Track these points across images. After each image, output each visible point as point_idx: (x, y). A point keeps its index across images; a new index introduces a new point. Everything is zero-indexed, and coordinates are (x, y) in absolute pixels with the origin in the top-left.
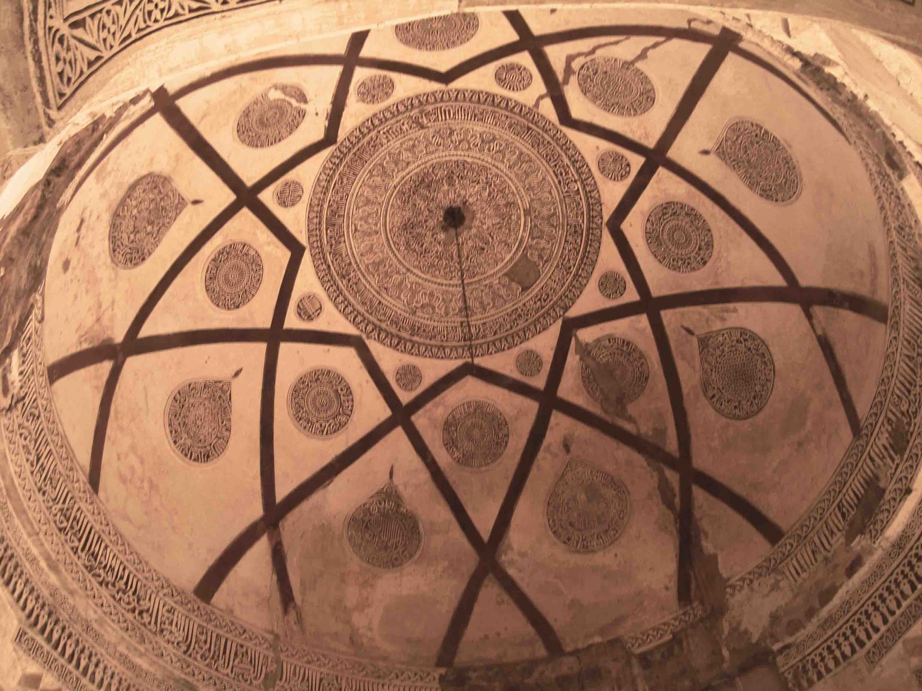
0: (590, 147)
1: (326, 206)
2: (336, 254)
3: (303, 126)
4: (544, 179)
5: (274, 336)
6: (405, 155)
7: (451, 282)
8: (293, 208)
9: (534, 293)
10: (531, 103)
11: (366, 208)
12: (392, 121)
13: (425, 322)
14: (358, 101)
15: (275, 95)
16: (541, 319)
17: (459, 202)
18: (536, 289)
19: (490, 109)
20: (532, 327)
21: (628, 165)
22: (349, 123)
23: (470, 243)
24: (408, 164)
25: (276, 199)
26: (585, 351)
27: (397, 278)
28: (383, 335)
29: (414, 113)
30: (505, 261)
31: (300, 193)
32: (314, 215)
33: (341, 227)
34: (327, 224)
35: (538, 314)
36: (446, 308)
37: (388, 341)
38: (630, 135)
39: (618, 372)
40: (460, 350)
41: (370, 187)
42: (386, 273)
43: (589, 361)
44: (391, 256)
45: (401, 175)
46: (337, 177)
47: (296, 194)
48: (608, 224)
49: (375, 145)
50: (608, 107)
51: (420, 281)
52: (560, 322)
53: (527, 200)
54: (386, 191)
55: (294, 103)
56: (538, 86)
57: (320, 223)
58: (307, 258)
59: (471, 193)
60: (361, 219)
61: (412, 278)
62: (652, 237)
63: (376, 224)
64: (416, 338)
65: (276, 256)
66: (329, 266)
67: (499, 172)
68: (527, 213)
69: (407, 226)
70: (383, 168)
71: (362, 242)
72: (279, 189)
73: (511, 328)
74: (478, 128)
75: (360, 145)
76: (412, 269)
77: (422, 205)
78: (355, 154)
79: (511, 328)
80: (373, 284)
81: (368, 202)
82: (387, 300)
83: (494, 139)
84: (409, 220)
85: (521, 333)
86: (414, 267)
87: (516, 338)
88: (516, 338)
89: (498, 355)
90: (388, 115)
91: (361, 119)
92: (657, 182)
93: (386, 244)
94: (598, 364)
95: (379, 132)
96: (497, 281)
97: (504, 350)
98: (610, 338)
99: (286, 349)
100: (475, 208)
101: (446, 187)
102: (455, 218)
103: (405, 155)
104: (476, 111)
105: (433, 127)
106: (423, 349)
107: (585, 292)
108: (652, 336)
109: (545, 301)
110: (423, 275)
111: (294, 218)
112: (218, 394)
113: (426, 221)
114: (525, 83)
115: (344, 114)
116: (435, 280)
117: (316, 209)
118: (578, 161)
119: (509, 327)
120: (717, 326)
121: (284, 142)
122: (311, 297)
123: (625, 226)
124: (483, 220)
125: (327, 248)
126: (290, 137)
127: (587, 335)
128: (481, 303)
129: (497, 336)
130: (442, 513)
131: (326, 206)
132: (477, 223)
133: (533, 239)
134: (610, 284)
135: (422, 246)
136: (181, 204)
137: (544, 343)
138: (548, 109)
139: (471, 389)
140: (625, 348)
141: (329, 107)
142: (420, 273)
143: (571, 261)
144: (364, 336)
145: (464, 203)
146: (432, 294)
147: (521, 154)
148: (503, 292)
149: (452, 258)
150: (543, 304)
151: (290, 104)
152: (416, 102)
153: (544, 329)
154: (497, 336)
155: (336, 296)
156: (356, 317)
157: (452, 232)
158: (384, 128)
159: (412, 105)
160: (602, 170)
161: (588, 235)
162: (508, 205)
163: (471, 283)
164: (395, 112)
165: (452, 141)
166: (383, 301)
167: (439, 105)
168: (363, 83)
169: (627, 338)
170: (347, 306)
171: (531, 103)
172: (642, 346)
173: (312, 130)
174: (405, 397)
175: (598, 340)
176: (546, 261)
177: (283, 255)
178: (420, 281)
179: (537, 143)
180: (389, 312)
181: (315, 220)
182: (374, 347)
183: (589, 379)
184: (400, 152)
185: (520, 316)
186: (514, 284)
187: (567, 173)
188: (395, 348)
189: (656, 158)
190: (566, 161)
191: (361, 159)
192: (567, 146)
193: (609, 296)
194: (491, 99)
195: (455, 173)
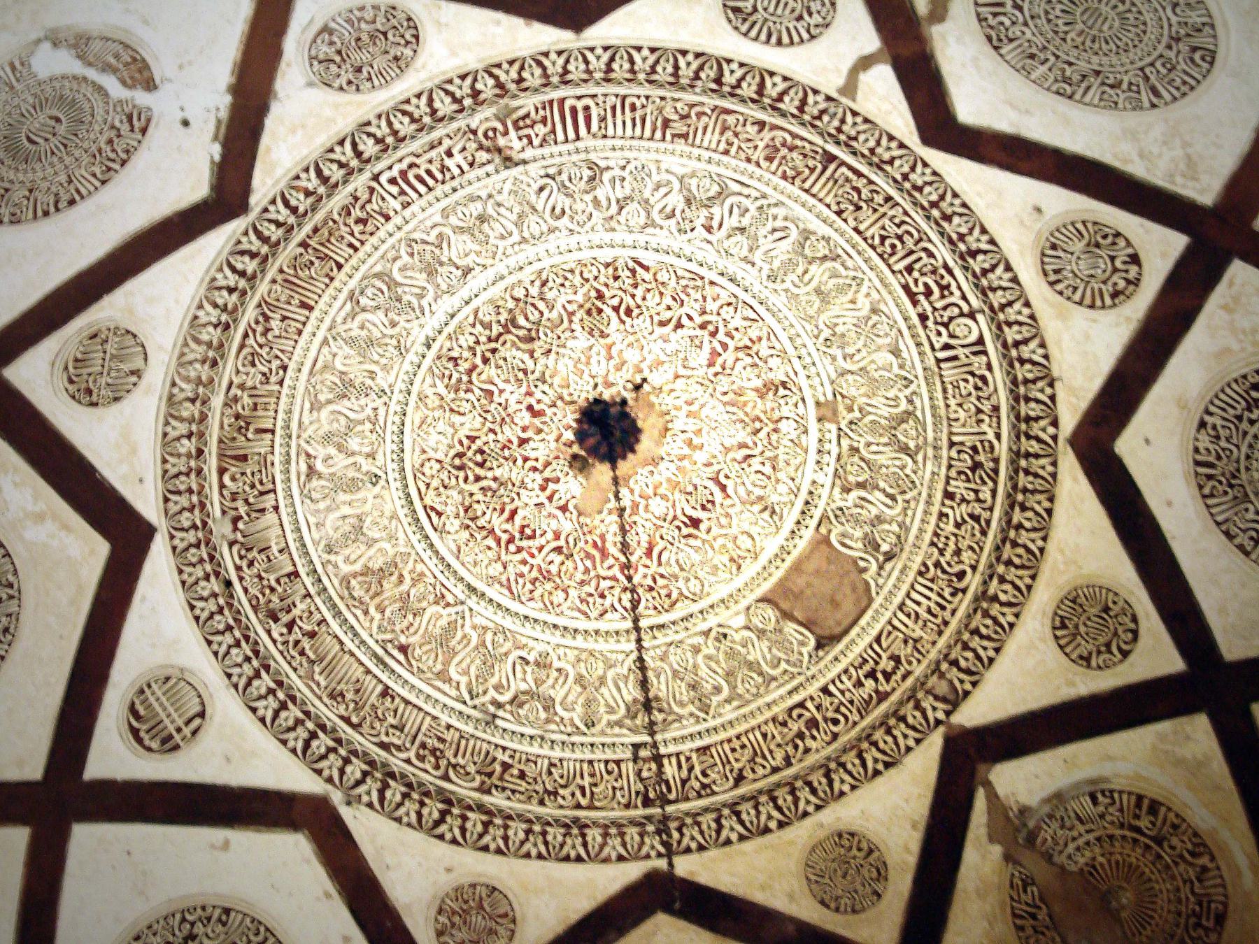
0: (1013, 208)
1: (217, 401)
2: (248, 547)
3: (140, 161)
4: (874, 311)
6: (460, 247)
7: (603, 625)
8: (116, 407)
9: (857, 650)
10: (831, 83)
11: (341, 406)
12: (415, 146)
13: (525, 747)
14: (311, 84)
15: (53, 63)
16: (879, 735)
18: (858, 643)
19: (711, 101)
20: (851, 759)
21: (1135, 259)
22: (281, 155)
23: (658, 506)
24: (467, 272)
25: (62, 382)
26: (1017, 831)
27: (435, 617)
28: (395, 792)
29: (482, 118)
30: (763, 559)
31: (138, 363)
32: (183, 428)
33: (265, 463)
34: (221, 456)
35: (868, 721)
36: (588, 703)
37: (411, 806)
38: (1137, 169)
39: (1127, 898)
40: (632, 832)
41: (351, 342)
42: (405, 599)
43: (1033, 864)
44: (420, 547)
45: (448, 303)
46: (250, 314)
47: (126, 367)
48: (1075, 442)
49: (364, 219)
50: (1068, 87)
51: (508, 622)
52: (935, 742)
53: (826, 369)
54: (402, 350)
55: (112, 85)
57: (200, 452)
58: (159, 564)
60: (327, 438)
61: (485, 614)
62: (1215, 476)
63: (372, 456)
64: (496, 800)
66: (228, 584)
67: (742, 295)
68: (826, 412)
69: (469, 460)
70: (392, 284)
71: (329, 510)
72: (73, 351)
73: (788, 761)
74: (674, 160)
75: (319, 216)
76: (481, 586)
77: (513, 395)
78: (304, 244)
79: (788, 761)
80: (365, 636)
81: (346, 387)
82: (410, 684)
83: (722, 194)
84: (472, 439)
85: (817, 778)
86: (491, 580)
87: (804, 794)
88: (804, 794)
89: (747, 846)
90: (404, 126)
91: (324, 139)
92: (1225, 308)
93: (401, 513)
94: (1062, 868)
95: (376, 178)
96: (740, 621)
97: (767, 830)
98: (1096, 791)
99: (89, 841)
100: (667, 401)
101: (582, 341)
102: (607, 431)
103: (460, 247)
104: (669, 113)
105: (541, 158)
106: (517, 830)
107: (1013, 645)
108: (1229, 783)
109: (888, 676)
110: (515, 606)
111: (123, 443)
113: (523, 442)
115: (269, 122)
116: (552, 619)
117: (188, 410)
118: (978, 252)
119: (779, 761)
121: (82, 208)
122: (171, 680)
123: (1129, 446)
125: (221, 529)
126: (106, 195)
127: (1020, 781)
128: (693, 687)
129: (742, 790)
131: (217, 401)
132: (673, 446)
133: (847, 490)
134: (1086, 623)
135: (514, 513)
137: (891, 808)
138: (884, 100)
140: (1144, 823)
141: (224, 101)
142: (507, 602)
143: (967, 556)
144: (337, 797)
145: (637, 388)
146: (542, 664)
147: (806, 234)
148: (759, 652)
149: (604, 554)
150: (884, 687)
151: (100, 89)
152: (487, 86)
153: (888, 765)
154: (742, 790)
155: (253, 676)
156: (313, 735)
157: (602, 472)
158: (392, 165)
159: (475, 94)
160: (1054, 279)
161: (1012, 478)
162: (769, 388)
163: (662, 626)
164: (424, 115)
165: (596, 201)
166: (397, 688)
167: (556, 95)
168: (326, 29)
169: (1151, 792)
170: (283, 706)
171: (831, 83)
172: (1200, 817)
173: (174, 170)
175: (1058, 798)
176: (889, 557)
177: (89, 551)
178: (508, 622)
179: (854, 203)
180: (412, 718)
181: (187, 446)
182: (369, 829)
184: (440, 236)
185: (812, 723)
186: (790, 627)
187: (944, 288)
188: (433, 830)
190: (943, 253)
191: (324, 258)
192: (944, 208)
193: (1086, 660)
194: (713, 72)
195: (608, 300)
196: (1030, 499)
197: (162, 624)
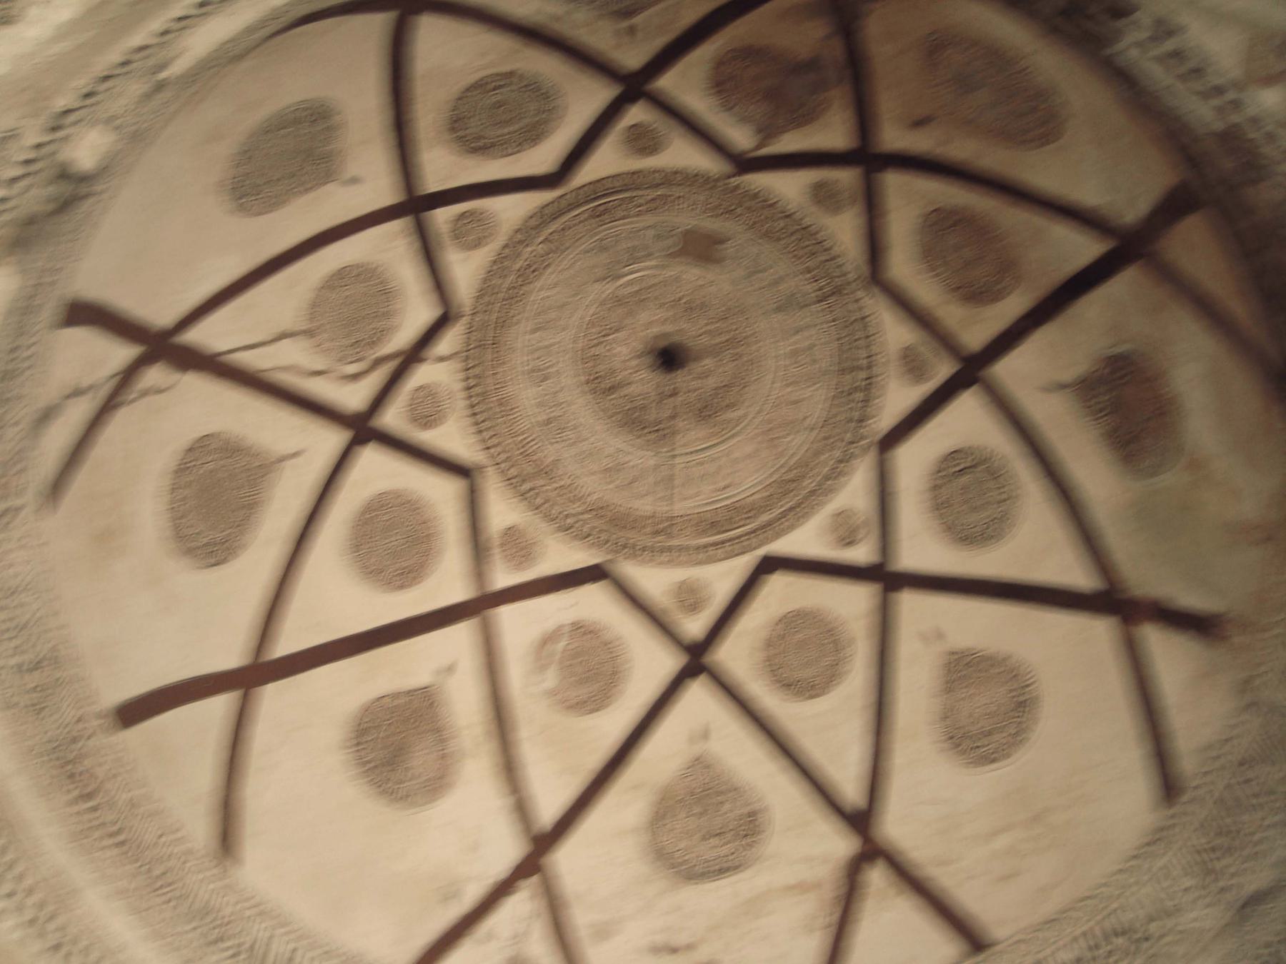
0: (465, 270)
5: (886, 578)
17: (648, 360)
26: (767, 132)
49: (598, 510)
56: (423, 375)
59: (625, 351)
62: (534, 135)
65: (781, 592)
74: (526, 396)
102: (669, 358)
111: (722, 578)
112: (963, 669)
114: (426, 392)
120: (582, 15)
124: (653, 323)
130: (1093, 308)
136: (700, 764)
138: (447, 343)
139: (903, 265)
174: (944, 370)
179: (503, 324)
183: (803, 117)
189: (415, 205)
192: (485, 291)
196: (599, 189)
197: (804, 540)
